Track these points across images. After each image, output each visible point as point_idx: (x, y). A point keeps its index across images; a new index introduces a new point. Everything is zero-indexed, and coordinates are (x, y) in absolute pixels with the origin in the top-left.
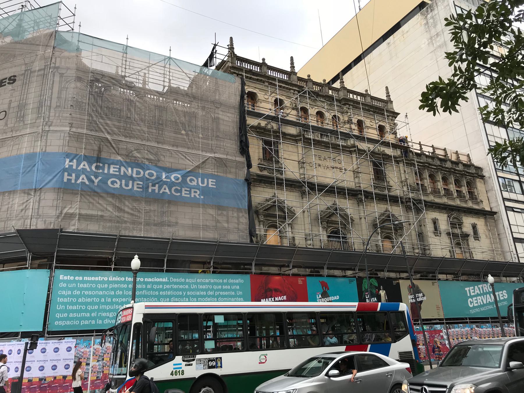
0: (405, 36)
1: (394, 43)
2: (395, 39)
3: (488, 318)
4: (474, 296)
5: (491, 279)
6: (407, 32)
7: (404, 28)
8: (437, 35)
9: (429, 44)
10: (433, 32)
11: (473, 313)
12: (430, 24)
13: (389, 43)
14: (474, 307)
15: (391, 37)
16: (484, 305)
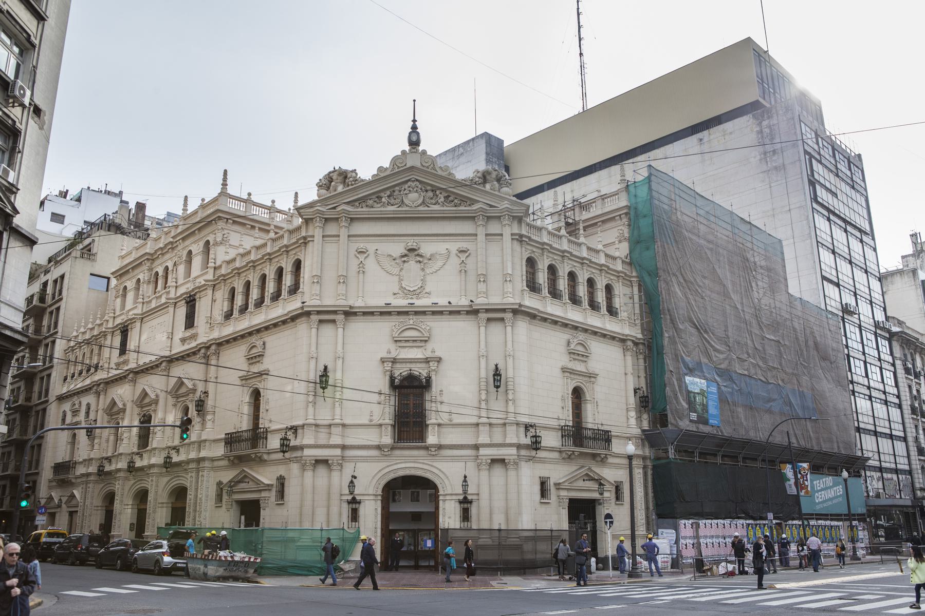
0: (727, 137)
1: (709, 141)
2: (712, 137)
3: (827, 515)
4: (821, 490)
5: (845, 474)
6: (731, 133)
7: (728, 126)
8: (774, 152)
9: (760, 160)
10: (769, 148)
11: (818, 509)
12: (765, 135)
13: (701, 140)
14: (820, 503)
15: (706, 133)
16: (826, 501)
